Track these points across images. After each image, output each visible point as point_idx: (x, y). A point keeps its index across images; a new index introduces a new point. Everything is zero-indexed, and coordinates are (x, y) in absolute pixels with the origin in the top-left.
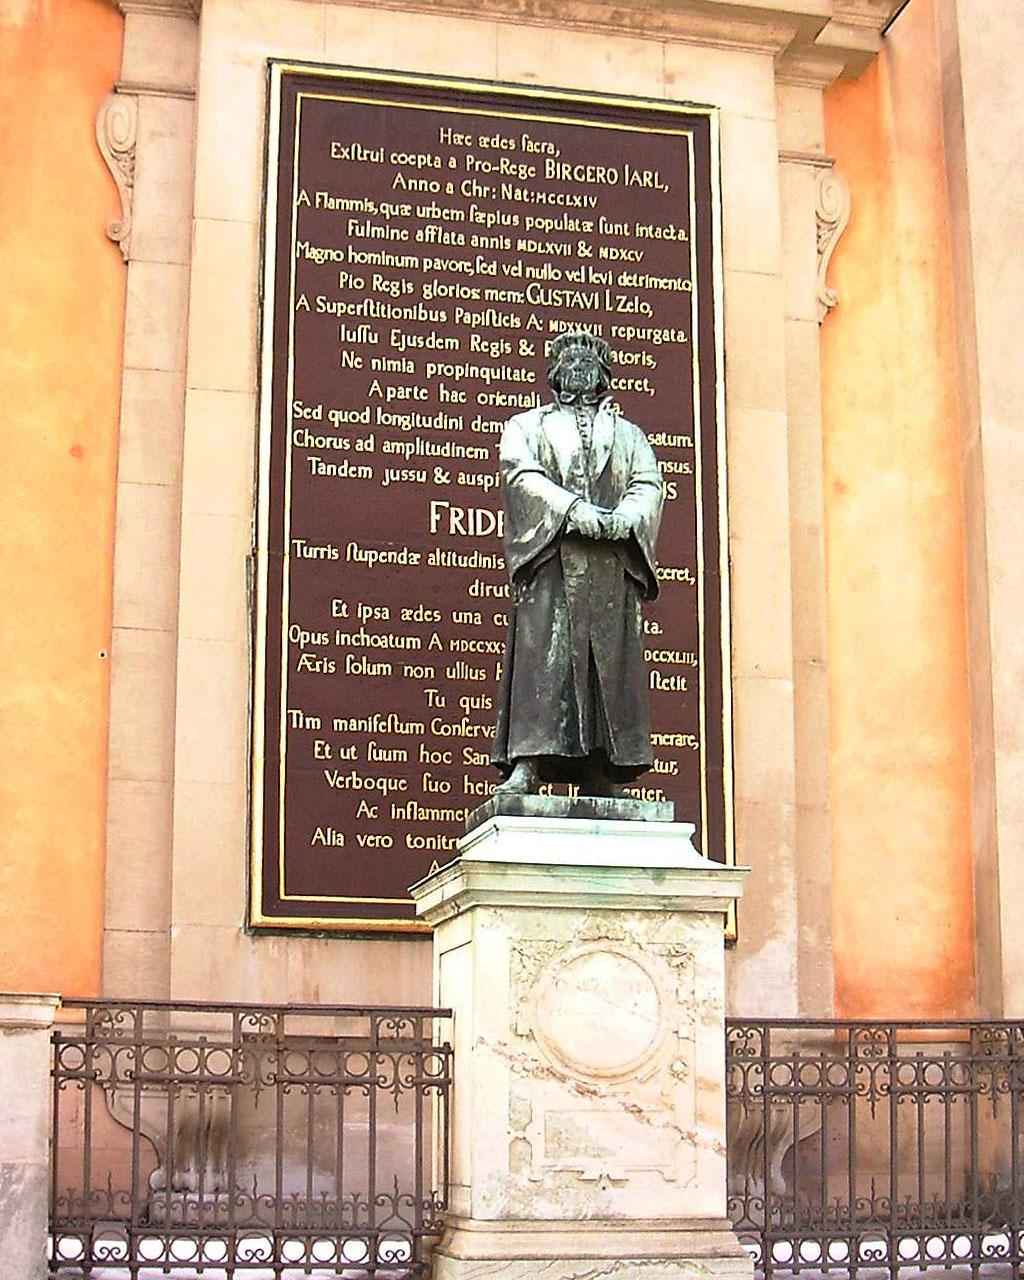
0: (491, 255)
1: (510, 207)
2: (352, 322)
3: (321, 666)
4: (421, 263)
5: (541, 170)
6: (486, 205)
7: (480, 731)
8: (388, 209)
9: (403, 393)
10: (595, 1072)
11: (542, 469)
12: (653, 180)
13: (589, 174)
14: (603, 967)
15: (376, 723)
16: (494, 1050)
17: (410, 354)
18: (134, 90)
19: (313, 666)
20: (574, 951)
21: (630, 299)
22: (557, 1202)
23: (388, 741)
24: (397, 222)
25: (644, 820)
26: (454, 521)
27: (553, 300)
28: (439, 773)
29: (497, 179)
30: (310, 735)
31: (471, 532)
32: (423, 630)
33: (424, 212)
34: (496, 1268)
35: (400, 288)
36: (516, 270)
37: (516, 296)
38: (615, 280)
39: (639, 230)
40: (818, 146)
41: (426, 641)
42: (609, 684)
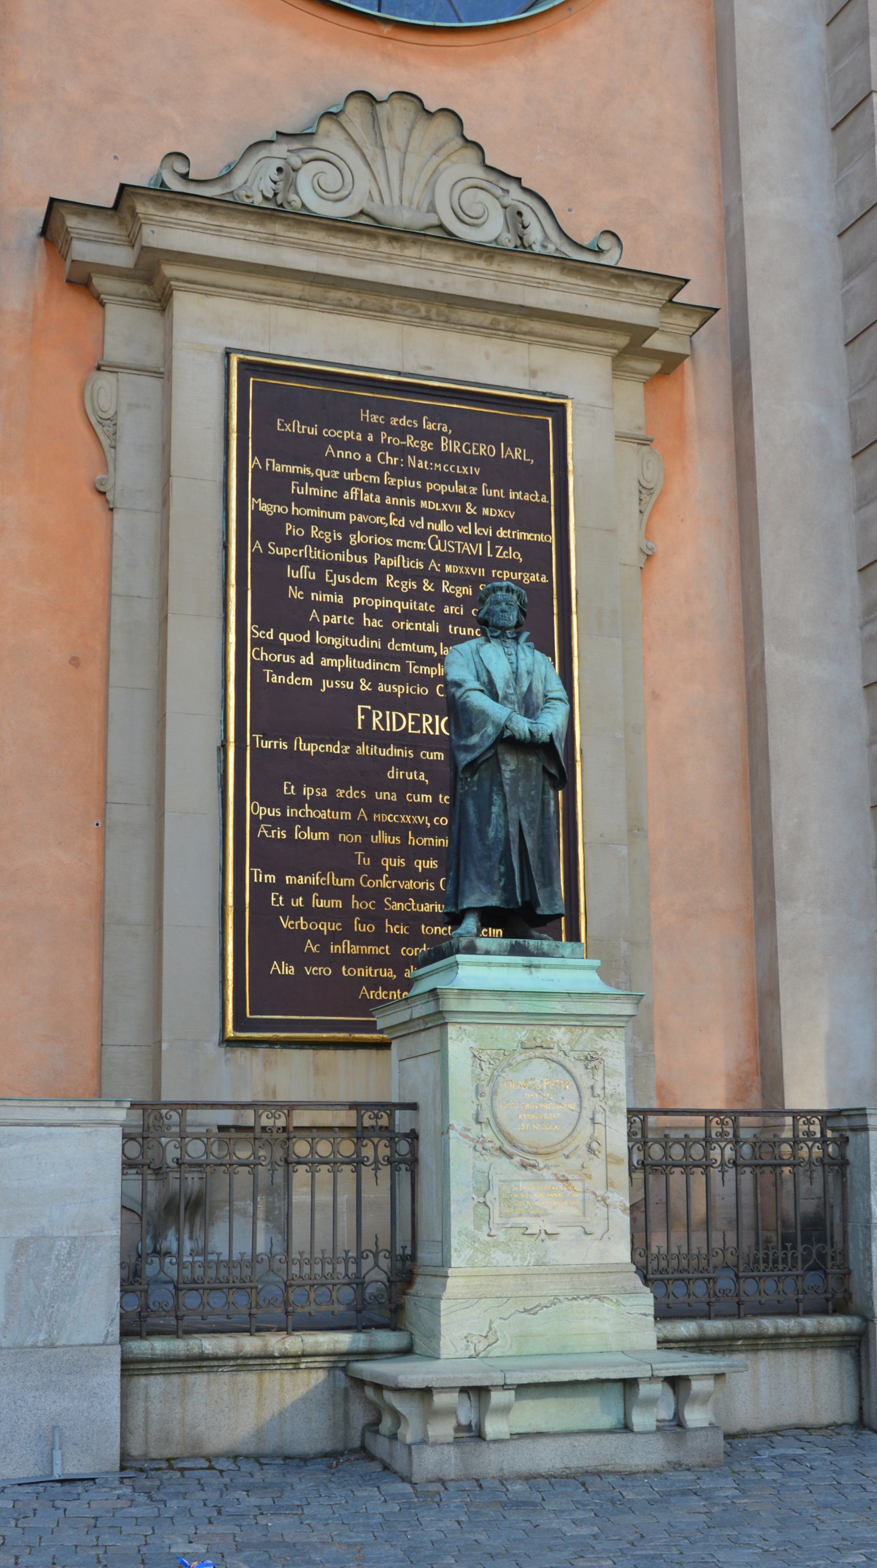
0: (401, 512)
1: (414, 474)
2: (296, 563)
3: (276, 834)
4: (348, 517)
5: (437, 445)
6: (397, 472)
7: (396, 884)
8: (322, 474)
9: (335, 620)
10: (535, 1150)
11: (482, 688)
12: (522, 455)
13: (474, 449)
15: (317, 878)
16: (461, 1135)
17: (341, 589)
18: (115, 368)
19: (270, 834)
21: (506, 548)
23: (326, 892)
24: (328, 484)
25: (563, 957)
26: (375, 720)
27: (448, 548)
29: (402, 452)
30: (269, 887)
31: (388, 729)
32: (353, 806)
33: (350, 476)
34: (466, 1305)
35: (332, 537)
36: (420, 524)
37: (419, 545)
38: (494, 533)
39: (512, 495)
40: (639, 428)
41: (355, 814)
42: (499, 849)
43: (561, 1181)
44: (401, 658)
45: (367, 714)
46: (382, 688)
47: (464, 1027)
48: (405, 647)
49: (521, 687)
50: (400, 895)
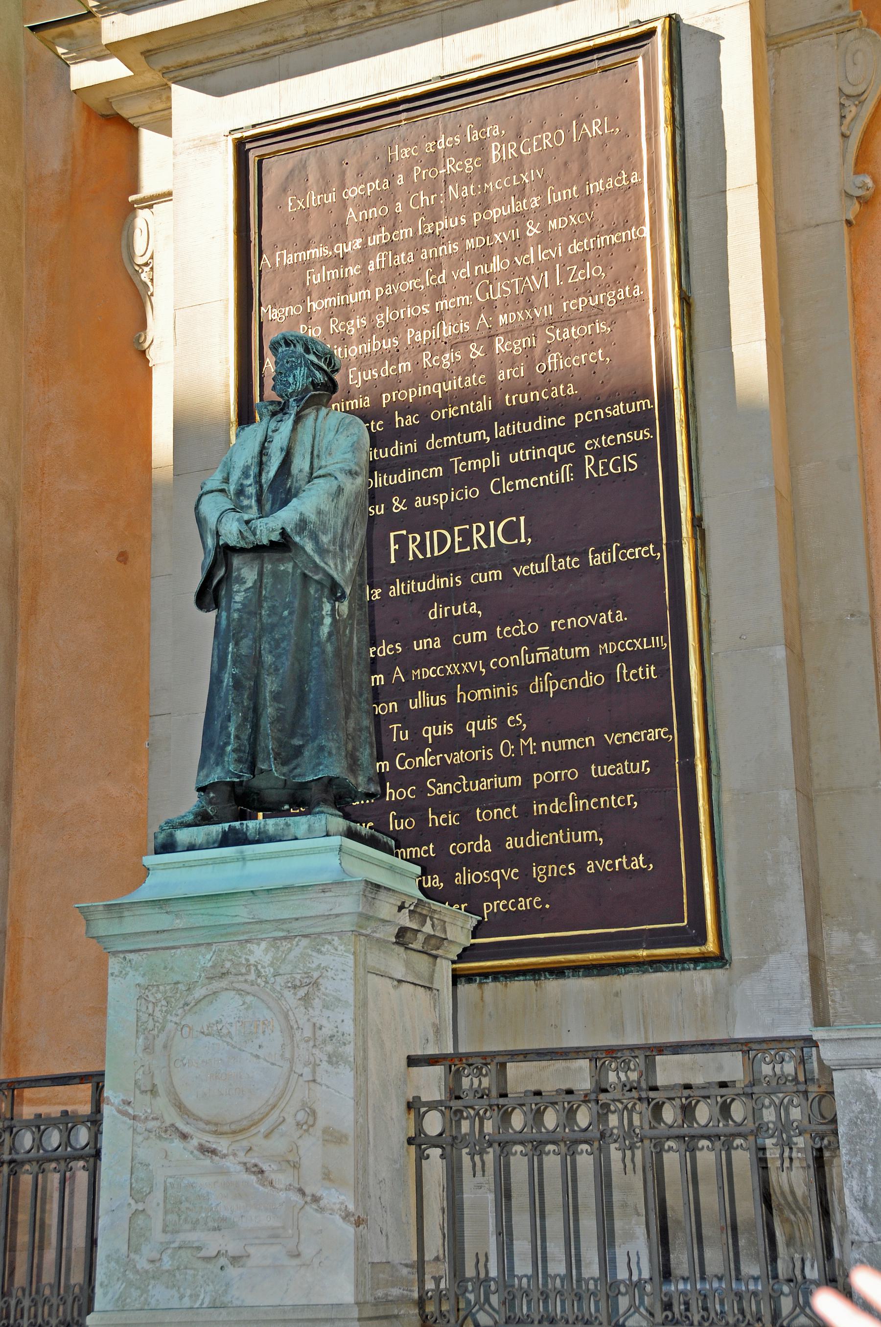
7: (443, 759)
14: (228, 1007)
16: (120, 1111)
20: (199, 993)
22: (174, 1286)
25: (296, 839)
26: (412, 546)
28: (404, 809)
31: (429, 555)
41: (388, 676)
43: (254, 1173)
44: (442, 457)
45: (402, 541)
46: (419, 502)
47: (130, 956)
48: (448, 440)
49: (268, 472)
50: (445, 773)
